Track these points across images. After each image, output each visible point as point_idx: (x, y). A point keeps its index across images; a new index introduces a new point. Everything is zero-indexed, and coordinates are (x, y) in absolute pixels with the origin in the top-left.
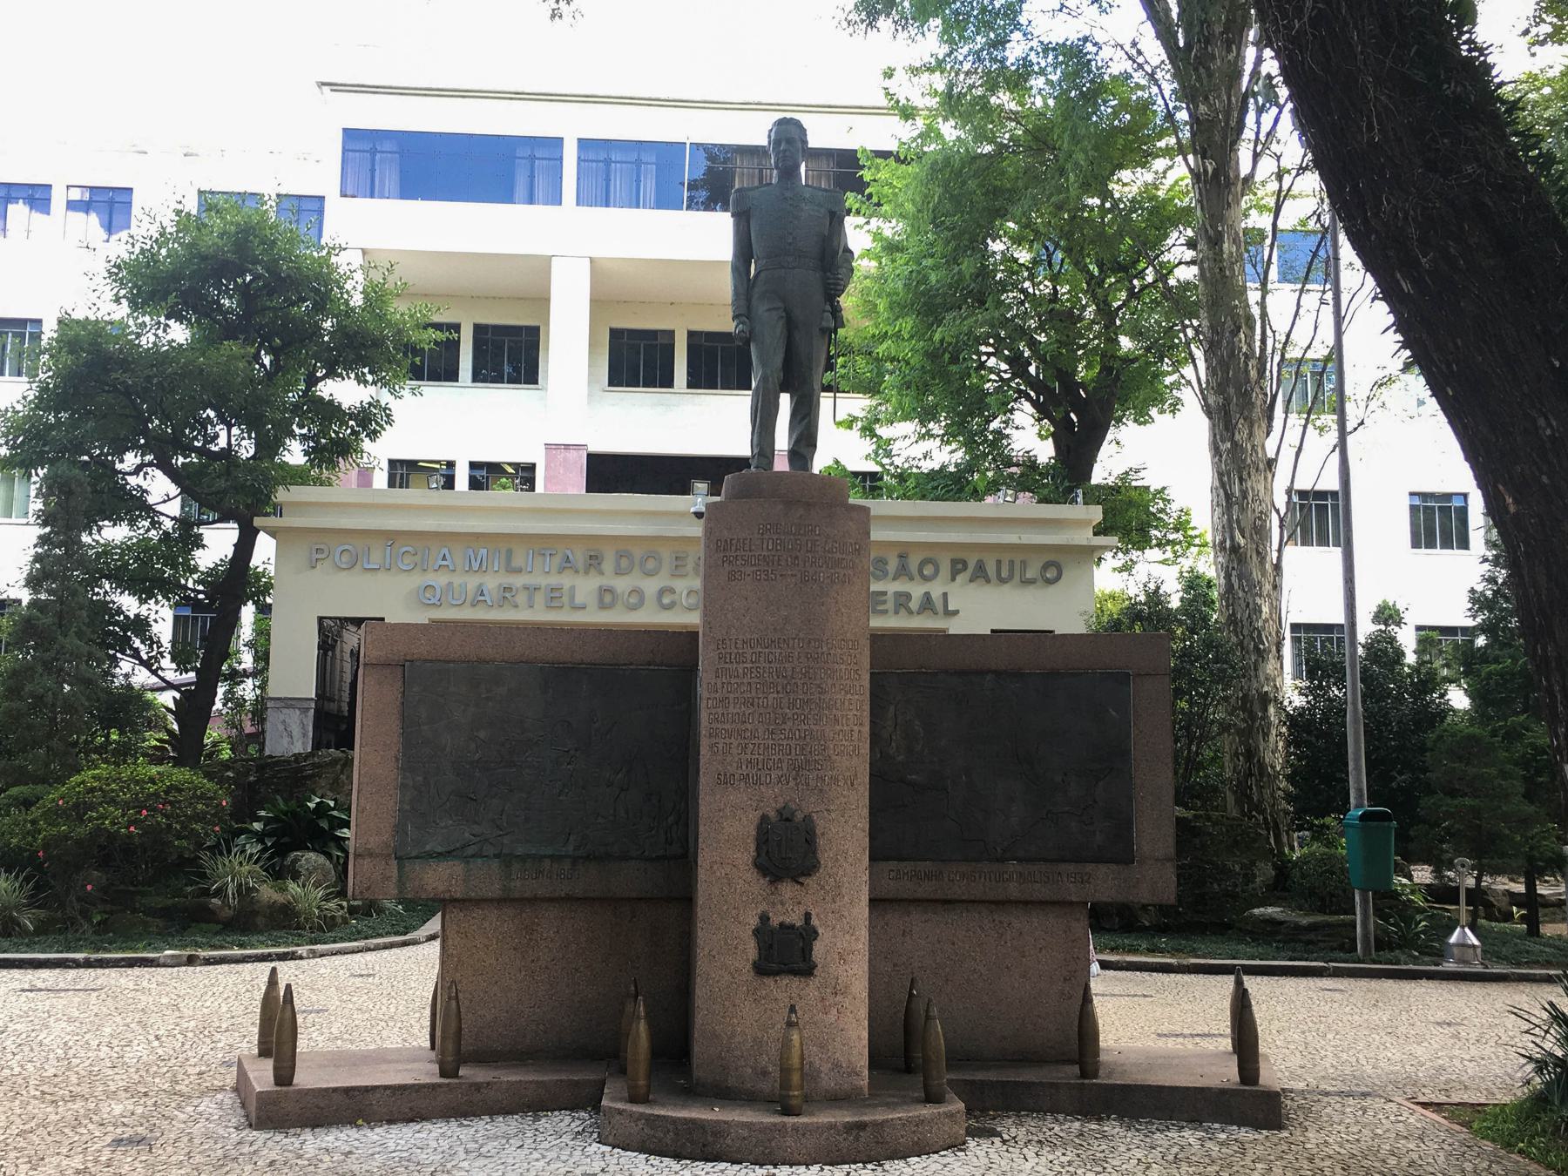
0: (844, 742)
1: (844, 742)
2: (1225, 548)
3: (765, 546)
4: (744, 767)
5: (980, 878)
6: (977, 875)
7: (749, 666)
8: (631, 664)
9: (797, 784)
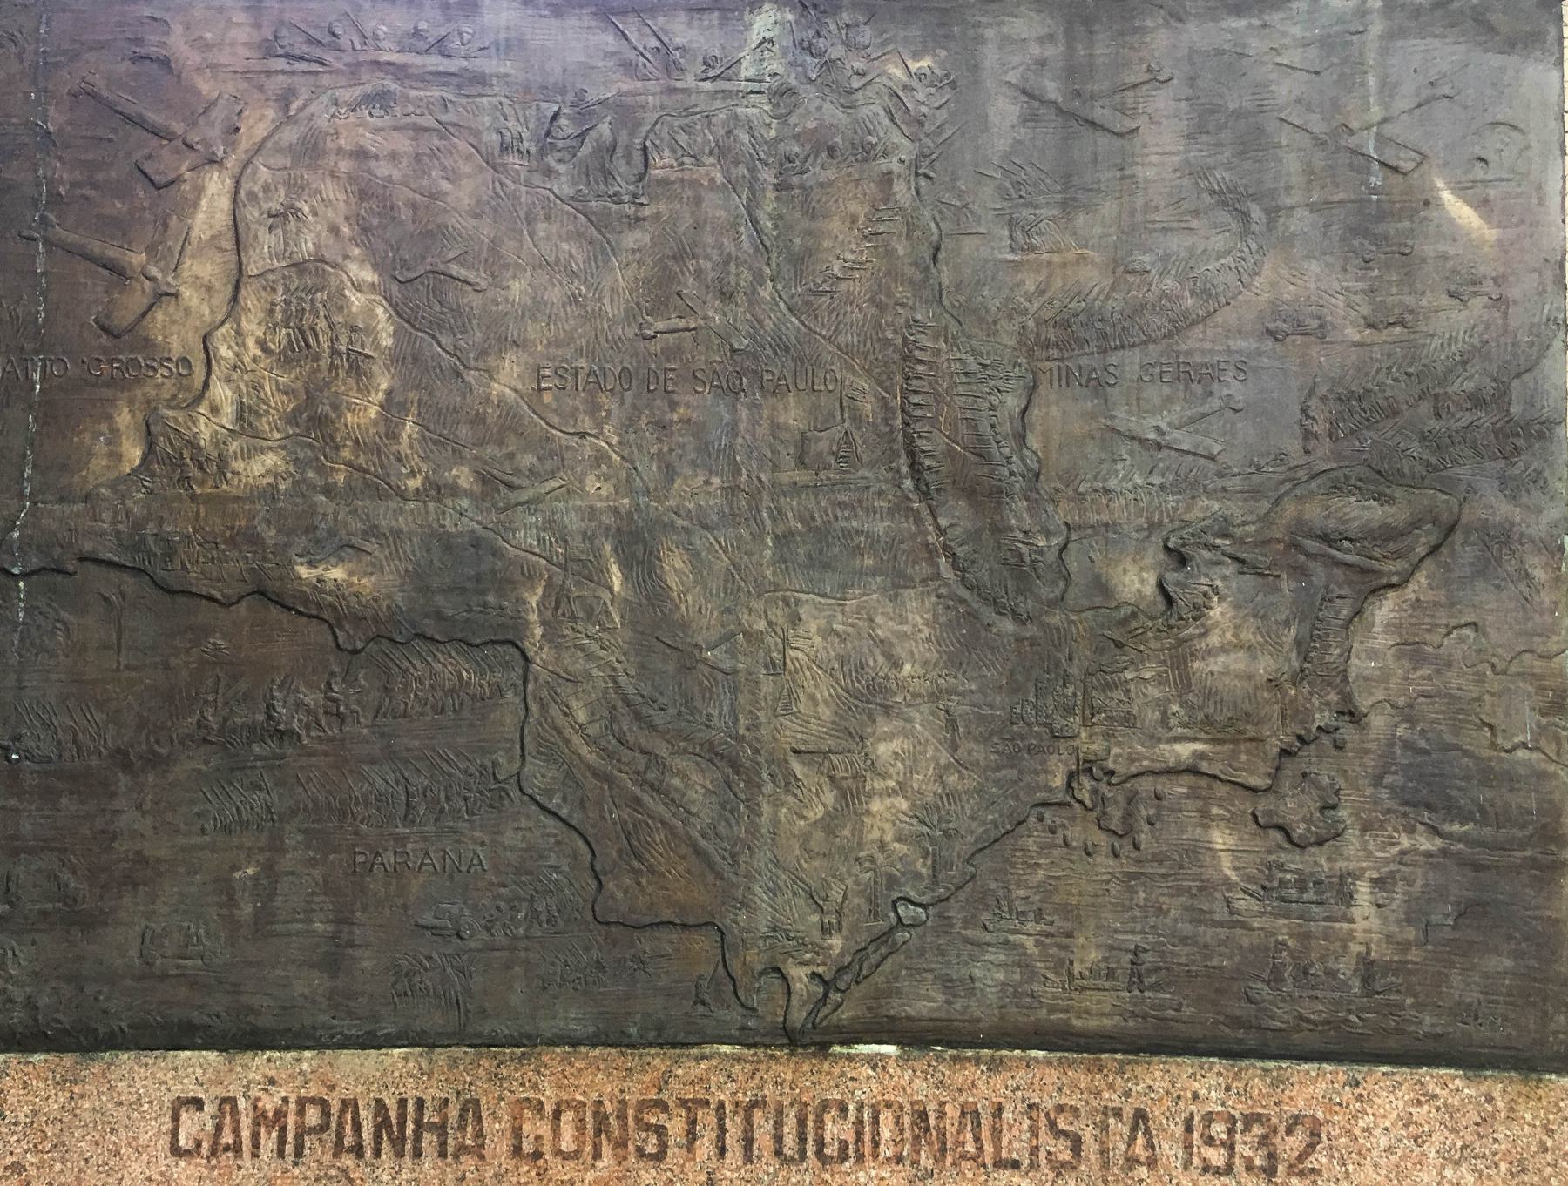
5: (692, 1136)
6: (676, 1126)
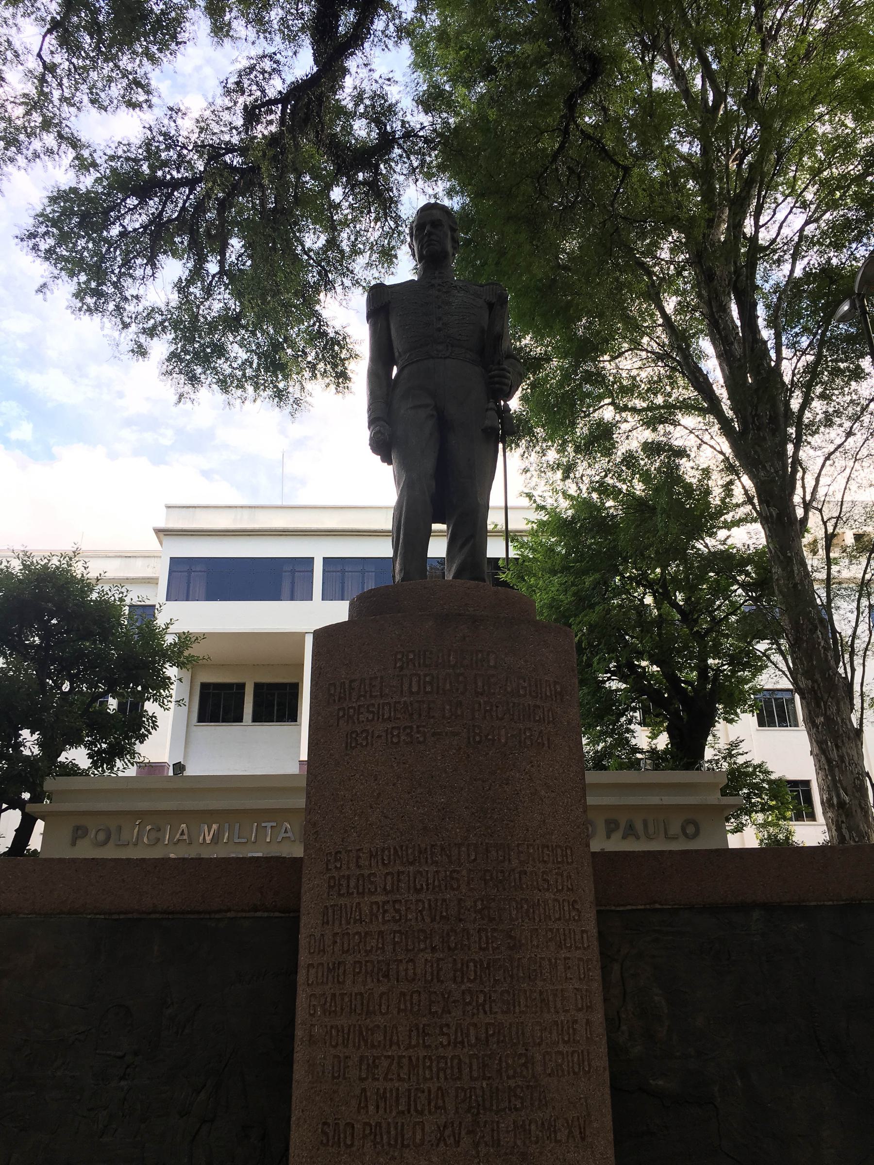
0: (561, 1047)
1: (561, 1047)
2: (833, 804)
3: (405, 688)
4: (371, 1108)
7: (380, 899)
8: (229, 910)
9: (476, 1145)
